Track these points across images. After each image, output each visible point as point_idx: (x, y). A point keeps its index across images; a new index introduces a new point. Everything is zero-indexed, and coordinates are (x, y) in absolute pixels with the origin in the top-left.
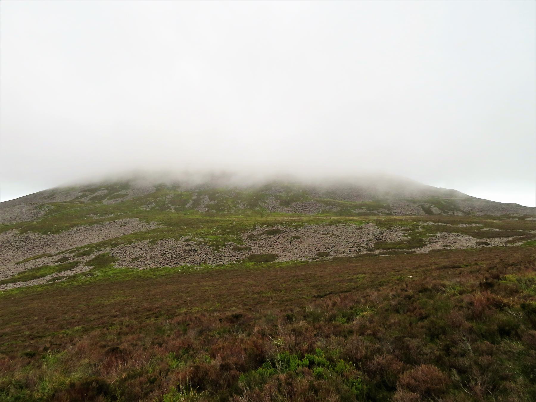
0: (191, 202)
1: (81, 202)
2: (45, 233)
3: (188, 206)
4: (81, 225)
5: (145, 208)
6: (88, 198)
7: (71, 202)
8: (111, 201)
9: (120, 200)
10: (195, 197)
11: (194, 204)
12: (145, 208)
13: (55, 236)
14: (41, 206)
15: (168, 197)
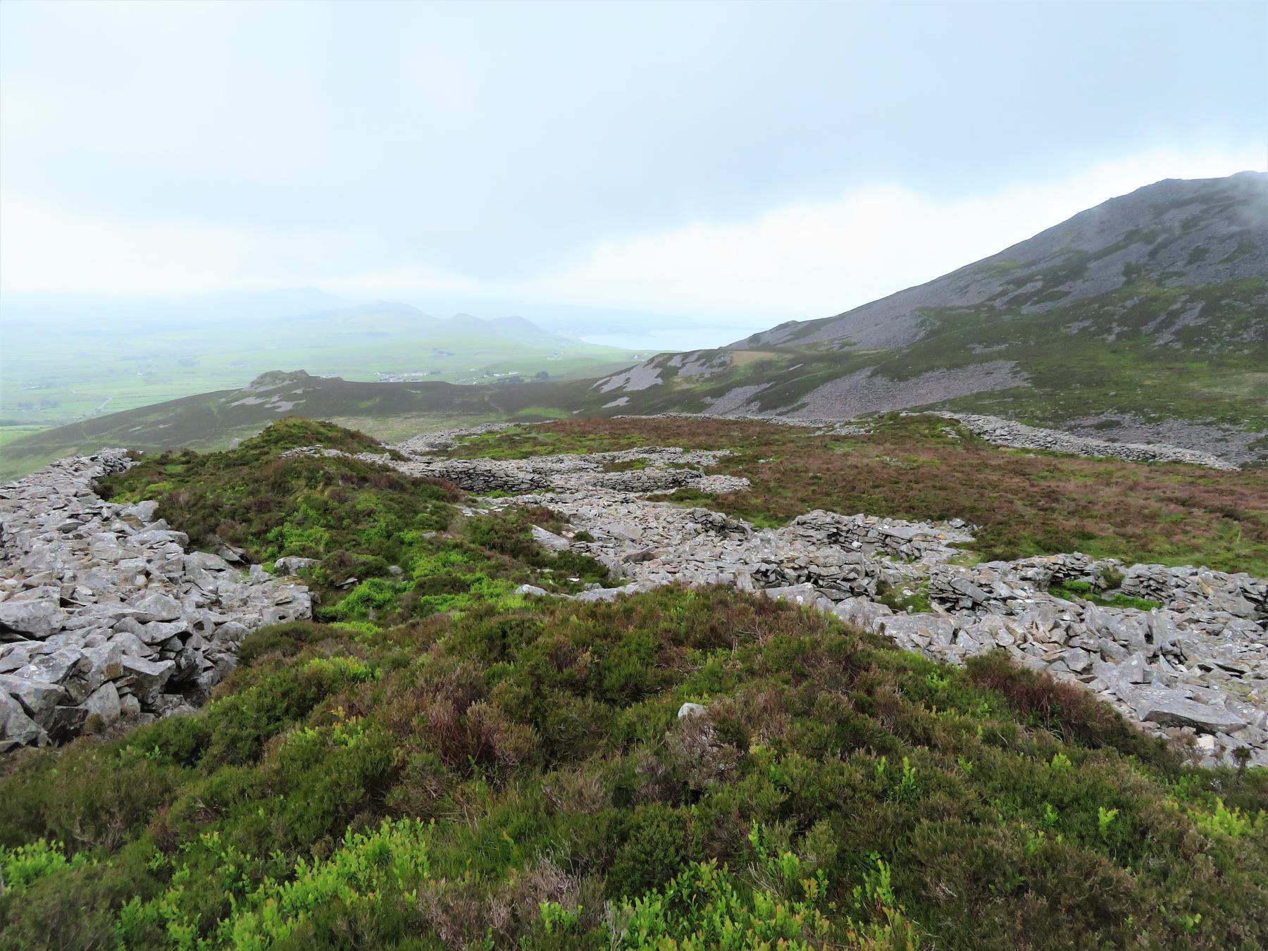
0: (1163, 316)
1: (992, 308)
2: (892, 380)
3: (1151, 326)
4: (938, 368)
5: (1074, 328)
6: (1006, 299)
7: (977, 308)
8: (1036, 309)
9: (1049, 305)
10: (1175, 307)
11: (1163, 321)
12: (1074, 328)
13: (902, 384)
14: (923, 323)
15: (1129, 303)
